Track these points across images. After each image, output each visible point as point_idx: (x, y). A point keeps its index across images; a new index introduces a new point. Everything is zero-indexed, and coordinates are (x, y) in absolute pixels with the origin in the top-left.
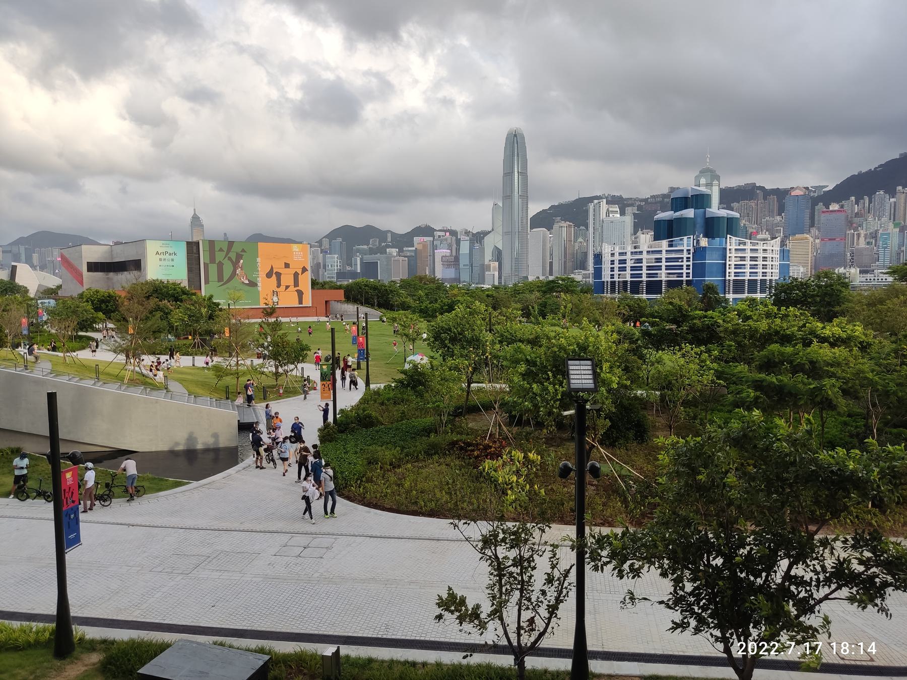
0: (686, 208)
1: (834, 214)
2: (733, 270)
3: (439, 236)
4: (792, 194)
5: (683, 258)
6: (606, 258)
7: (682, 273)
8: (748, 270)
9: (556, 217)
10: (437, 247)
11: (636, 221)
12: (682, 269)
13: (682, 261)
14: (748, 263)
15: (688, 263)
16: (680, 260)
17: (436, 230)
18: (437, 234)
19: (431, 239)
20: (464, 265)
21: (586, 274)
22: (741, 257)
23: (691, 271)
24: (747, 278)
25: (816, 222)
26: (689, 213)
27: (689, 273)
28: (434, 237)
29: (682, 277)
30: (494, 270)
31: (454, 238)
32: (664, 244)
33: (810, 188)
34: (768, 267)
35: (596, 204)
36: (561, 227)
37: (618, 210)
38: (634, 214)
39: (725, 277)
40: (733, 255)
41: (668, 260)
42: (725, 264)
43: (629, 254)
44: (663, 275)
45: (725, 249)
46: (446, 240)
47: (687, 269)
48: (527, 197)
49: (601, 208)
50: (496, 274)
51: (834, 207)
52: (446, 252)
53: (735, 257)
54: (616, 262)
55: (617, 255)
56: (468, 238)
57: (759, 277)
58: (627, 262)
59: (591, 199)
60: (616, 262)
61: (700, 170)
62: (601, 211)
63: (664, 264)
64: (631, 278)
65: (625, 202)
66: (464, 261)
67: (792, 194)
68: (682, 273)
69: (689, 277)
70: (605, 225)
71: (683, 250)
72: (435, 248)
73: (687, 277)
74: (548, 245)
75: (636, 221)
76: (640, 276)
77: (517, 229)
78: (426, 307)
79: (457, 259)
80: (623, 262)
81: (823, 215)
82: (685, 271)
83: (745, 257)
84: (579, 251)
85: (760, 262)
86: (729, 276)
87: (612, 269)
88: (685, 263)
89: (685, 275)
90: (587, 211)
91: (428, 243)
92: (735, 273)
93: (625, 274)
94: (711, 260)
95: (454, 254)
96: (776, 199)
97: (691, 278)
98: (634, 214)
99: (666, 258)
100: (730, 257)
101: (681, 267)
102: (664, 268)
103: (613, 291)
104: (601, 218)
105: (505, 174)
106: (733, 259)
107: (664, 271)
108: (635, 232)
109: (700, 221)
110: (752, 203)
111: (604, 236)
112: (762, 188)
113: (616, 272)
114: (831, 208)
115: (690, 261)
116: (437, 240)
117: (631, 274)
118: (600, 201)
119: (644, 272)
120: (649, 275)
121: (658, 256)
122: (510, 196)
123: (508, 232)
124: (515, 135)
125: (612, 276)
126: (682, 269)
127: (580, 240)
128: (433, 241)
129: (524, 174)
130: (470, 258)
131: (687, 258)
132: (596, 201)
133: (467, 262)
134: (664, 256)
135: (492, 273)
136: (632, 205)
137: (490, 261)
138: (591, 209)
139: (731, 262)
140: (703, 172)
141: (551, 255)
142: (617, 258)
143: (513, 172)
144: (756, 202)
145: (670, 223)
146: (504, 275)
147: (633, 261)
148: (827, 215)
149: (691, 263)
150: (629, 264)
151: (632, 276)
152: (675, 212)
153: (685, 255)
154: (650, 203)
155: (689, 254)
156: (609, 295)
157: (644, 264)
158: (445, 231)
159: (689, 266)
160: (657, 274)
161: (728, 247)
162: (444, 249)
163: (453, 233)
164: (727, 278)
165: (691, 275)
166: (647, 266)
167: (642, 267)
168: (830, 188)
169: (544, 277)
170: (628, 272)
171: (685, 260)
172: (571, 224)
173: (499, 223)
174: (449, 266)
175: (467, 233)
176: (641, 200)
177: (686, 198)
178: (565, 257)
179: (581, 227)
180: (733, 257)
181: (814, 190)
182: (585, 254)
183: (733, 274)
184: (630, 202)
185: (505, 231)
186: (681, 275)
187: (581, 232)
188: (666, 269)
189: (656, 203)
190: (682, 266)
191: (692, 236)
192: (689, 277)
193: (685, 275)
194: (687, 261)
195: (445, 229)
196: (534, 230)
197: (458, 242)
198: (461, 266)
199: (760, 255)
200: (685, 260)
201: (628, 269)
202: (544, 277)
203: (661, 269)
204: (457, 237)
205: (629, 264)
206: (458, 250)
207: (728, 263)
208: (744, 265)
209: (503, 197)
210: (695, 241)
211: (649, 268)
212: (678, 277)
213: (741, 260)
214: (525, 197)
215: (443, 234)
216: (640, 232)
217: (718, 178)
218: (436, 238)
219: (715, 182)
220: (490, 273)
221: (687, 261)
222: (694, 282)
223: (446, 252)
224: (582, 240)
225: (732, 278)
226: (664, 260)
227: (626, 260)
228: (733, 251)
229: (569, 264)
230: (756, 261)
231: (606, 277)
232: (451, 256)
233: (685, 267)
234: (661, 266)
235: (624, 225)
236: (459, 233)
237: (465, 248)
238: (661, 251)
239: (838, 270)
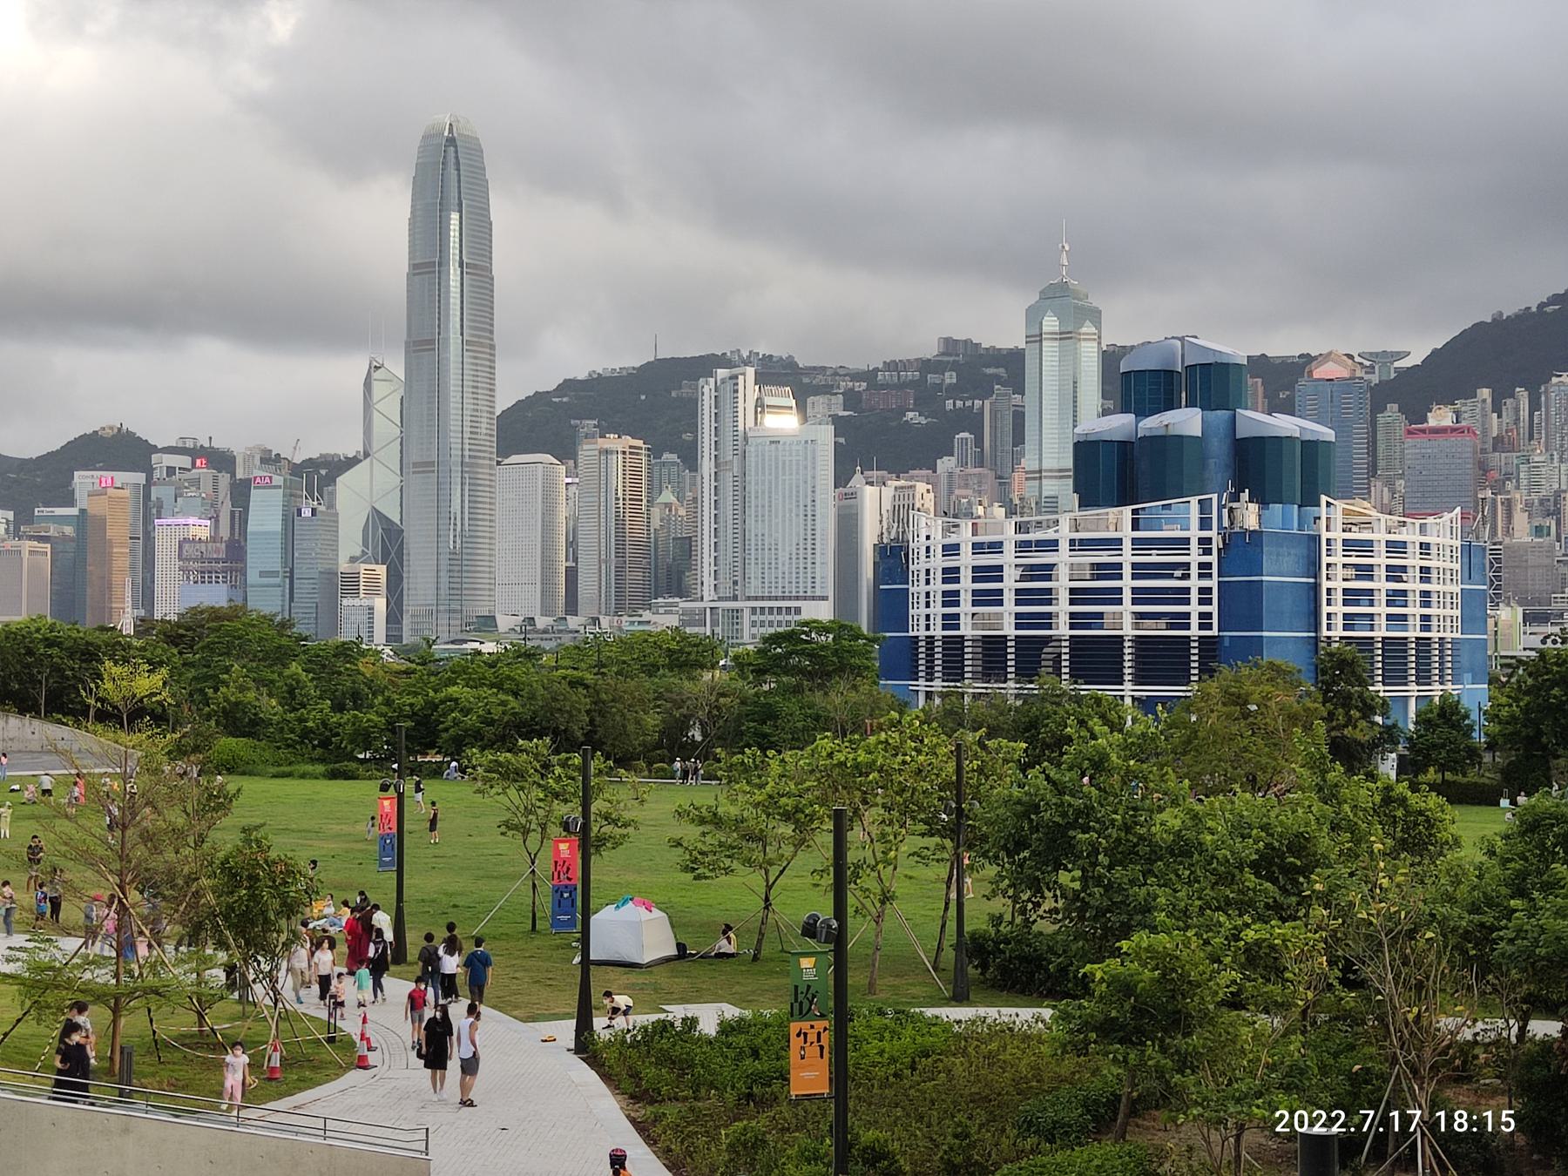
0: (1171, 405)
1: (1441, 441)
2: (1339, 609)
3: (171, 471)
4: (1316, 375)
5: (1187, 566)
6: (926, 563)
7: (1187, 615)
8: (1381, 609)
9: (581, 419)
10: (160, 507)
11: (842, 440)
12: (1187, 602)
13: (1186, 577)
14: (1381, 585)
15: (1205, 583)
16: (1178, 573)
17: (155, 449)
18: (163, 461)
19: (140, 478)
20: (262, 574)
21: (691, 612)
22: (1357, 567)
23: (1213, 609)
24: (1381, 632)
25: (1381, 464)
26: (1187, 421)
27: (1209, 615)
28: (149, 470)
29: (1187, 627)
30: (372, 592)
31: (224, 479)
32: (1118, 520)
34: (1410, 598)
35: (723, 381)
39: (1317, 628)
40: (1338, 559)
41: (1140, 571)
42: (1316, 588)
43: (1009, 548)
44: (1124, 621)
45: (1316, 539)
46: (196, 483)
47: (1201, 602)
48: (492, 347)
49: (740, 394)
50: (380, 604)
51: (1441, 417)
52: (200, 528)
53: (1345, 566)
54: (966, 576)
55: (966, 549)
56: (278, 480)
57: (1413, 633)
58: (1005, 574)
59: (704, 365)
60: (966, 576)
61: (1040, 290)
62: (740, 410)
63: (1127, 583)
64: (1018, 626)
65: (806, 380)
66: (262, 558)
67: (1316, 375)
68: (1187, 615)
69: (1209, 627)
70: (751, 449)
71: (1187, 541)
72: (149, 510)
73: (1202, 627)
74: (563, 512)
75: (842, 440)
76: (1046, 620)
77: (456, 452)
78: (324, 724)
79: (236, 551)
80: (995, 573)
81: (1410, 441)
82: (1194, 608)
83: (1370, 567)
84: (662, 534)
85: (1413, 585)
86: (1329, 629)
87: (951, 599)
88: (1194, 583)
89: (1194, 621)
91: (126, 493)
92: (1346, 616)
93: (1000, 616)
94: (1278, 574)
95: (225, 533)
96: (1260, 390)
97: (1215, 632)
98: (836, 420)
99: (1134, 566)
100: (1329, 565)
101: (1182, 595)
102: (1127, 596)
103: (954, 670)
104: (741, 428)
105: (414, 265)
106: (1340, 572)
107: (1128, 607)
108: (841, 479)
109: (1219, 450)
111: (751, 488)
113: (966, 607)
114: (1433, 421)
115: (1210, 575)
116: (161, 482)
117: (1018, 616)
118: (735, 371)
119: (1063, 608)
120: (1076, 620)
121: (1105, 558)
122: (432, 342)
124: (451, 141)
125: (951, 621)
126: (1187, 602)
127: (668, 496)
128: (148, 486)
129: (479, 270)
130: (285, 549)
131: (1202, 566)
132: (722, 373)
133: (276, 564)
134: (1127, 557)
135: (365, 602)
136: (827, 390)
137: (353, 560)
138: (706, 397)
139: (1335, 582)
140: (1055, 295)
141: (572, 544)
142: (966, 560)
143: (443, 263)
145: (1125, 450)
146: (410, 606)
147: (1019, 572)
148: (1420, 440)
149: (1213, 583)
150: (1010, 582)
151: (1022, 621)
152: (1141, 413)
153: (1194, 557)
155: (1208, 552)
156: (938, 685)
157: (1062, 584)
158: (195, 452)
159: (1209, 590)
160: (1100, 615)
161: (1325, 535)
162: (186, 515)
163: (221, 460)
164: (1325, 633)
165: (1215, 621)
166: (1072, 591)
167: (1000, 592)
168: (1415, 359)
169: (550, 621)
170: (1009, 607)
171: (1194, 571)
172: (639, 443)
173: (387, 427)
174: (205, 575)
175: (270, 459)
176: (856, 376)
177: (1169, 374)
178: (620, 553)
179: (668, 457)
180: (1340, 567)
181: (1367, 363)
182: (687, 547)
183: (1339, 621)
184: (819, 380)
185: (415, 456)
186: (1182, 620)
188: (1135, 602)
189: (902, 386)
190: (1187, 590)
191: (1215, 497)
192: (1209, 627)
193: (1194, 621)
194: (1201, 576)
195: (190, 444)
196: (514, 459)
197: (241, 492)
198: (252, 577)
199: (1413, 561)
200: (1194, 571)
201: (1009, 597)
202: (550, 621)
203: (1119, 602)
204: (233, 474)
205: (1010, 582)
206: (240, 519)
207: (1325, 584)
208: (1370, 592)
209: (407, 344)
210: (1225, 511)
211: (1077, 595)
212: (1171, 627)
213: (1358, 578)
214: (482, 340)
215: (185, 461)
217: (1095, 316)
218: (157, 474)
219: (1088, 328)
220: (356, 602)
221: (1201, 576)
222: (1227, 643)
223: (200, 528)
224: (673, 499)
225: (1338, 632)
226: (1127, 571)
227: (1000, 568)
228: (1339, 547)
229: (634, 576)
230: (1371, 578)
231: (926, 619)
232: (214, 539)
233: (1194, 596)
234: (1119, 590)
235: (814, 451)
236: (239, 461)
237: (265, 514)
238: (1055, 543)
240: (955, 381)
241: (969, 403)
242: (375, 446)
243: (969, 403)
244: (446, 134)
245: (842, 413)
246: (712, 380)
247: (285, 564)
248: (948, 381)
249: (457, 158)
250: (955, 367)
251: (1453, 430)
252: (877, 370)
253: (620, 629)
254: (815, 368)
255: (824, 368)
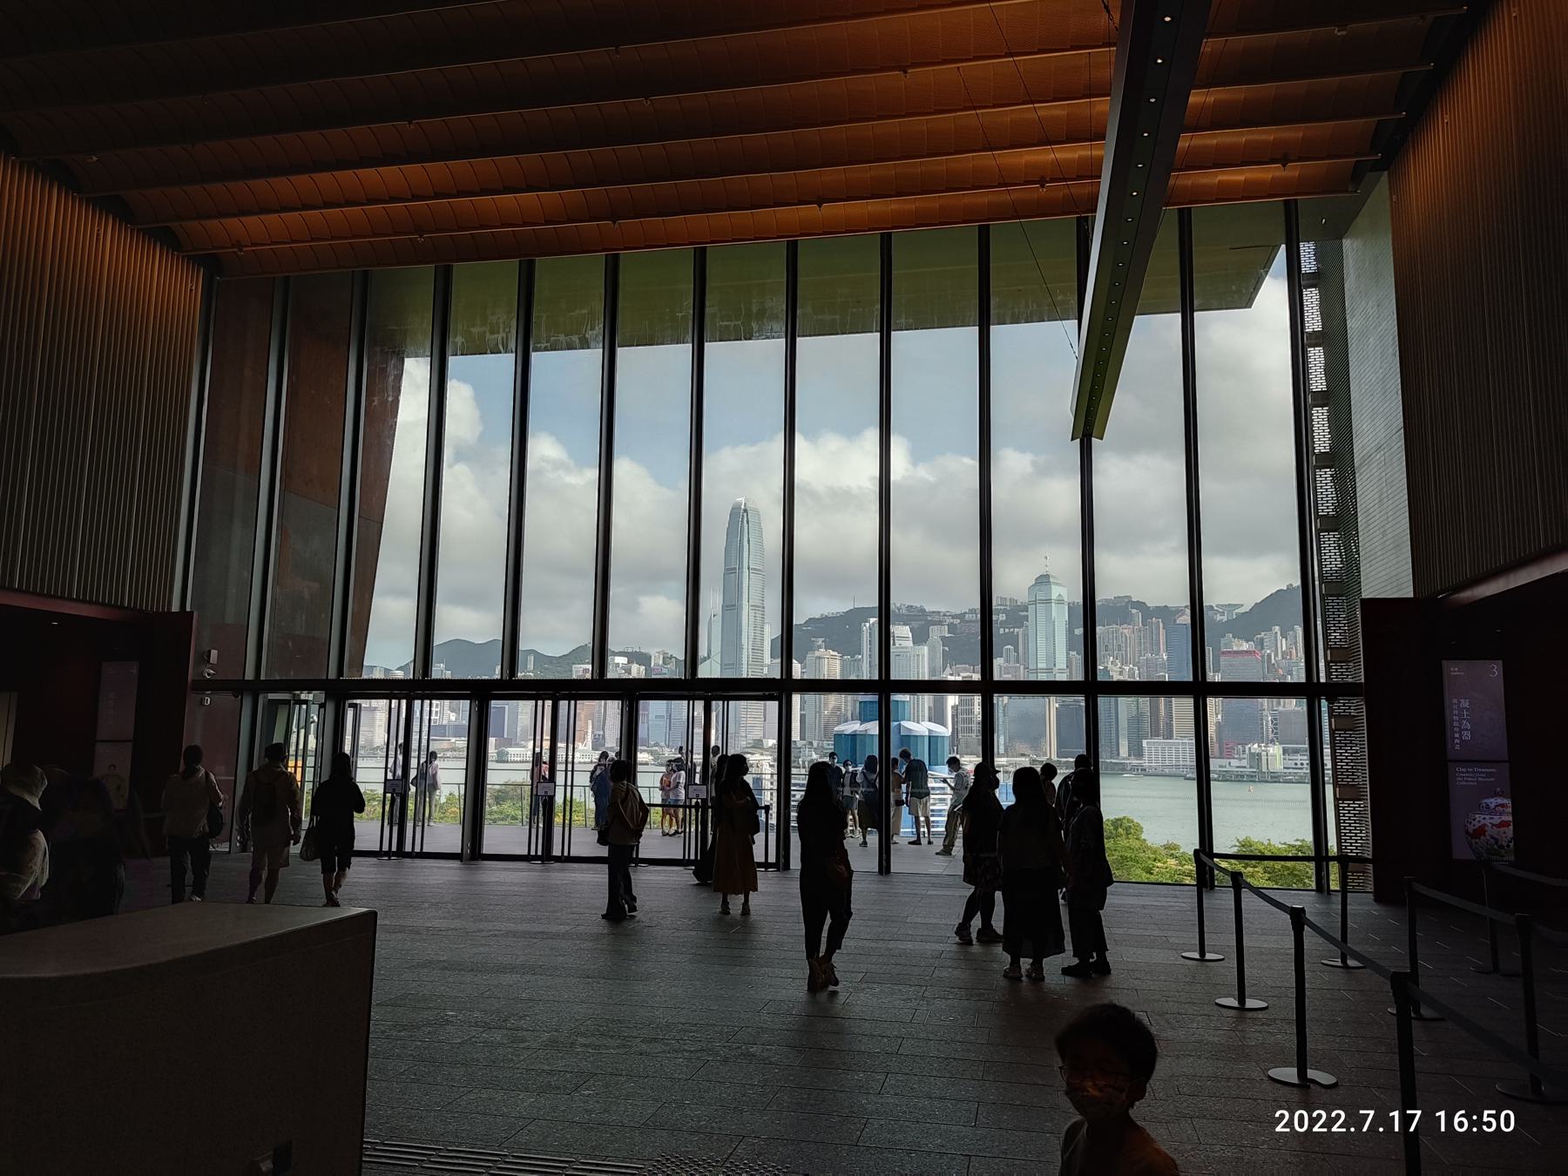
33: (1216, 608)
36: (819, 658)
37: (910, 635)
38: (943, 638)
48: (763, 608)
65: (929, 618)
75: (947, 649)
90: (860, 631)
110: (1126, 630)
112: (1140, 605)
122: (734, 605)
123: (730, 664)
136: (940, 623)
138: (865, 633)
144: (1131, 627)
154: (968, 622)
168: (1246, 609)
172: (836, 653)
176: (954, 617)
184: (937, 618)
187: (856, 664)
216: (948, 669)
239: (1250, 748)
240: (1004, 618)
241: (1012, 630)
242: (712, 655)
243: (1012, 630)
244: (743, 507)
245: (947, 635)
246: (868, 625)
247: (667, 711)
248: (1001, 619)
249: (747, 519)
250: (1005, 611)
251: (1247, 652)
252: (966, 613)
253: (822, 747)
254: (934, 612)
255: (939, 612)
